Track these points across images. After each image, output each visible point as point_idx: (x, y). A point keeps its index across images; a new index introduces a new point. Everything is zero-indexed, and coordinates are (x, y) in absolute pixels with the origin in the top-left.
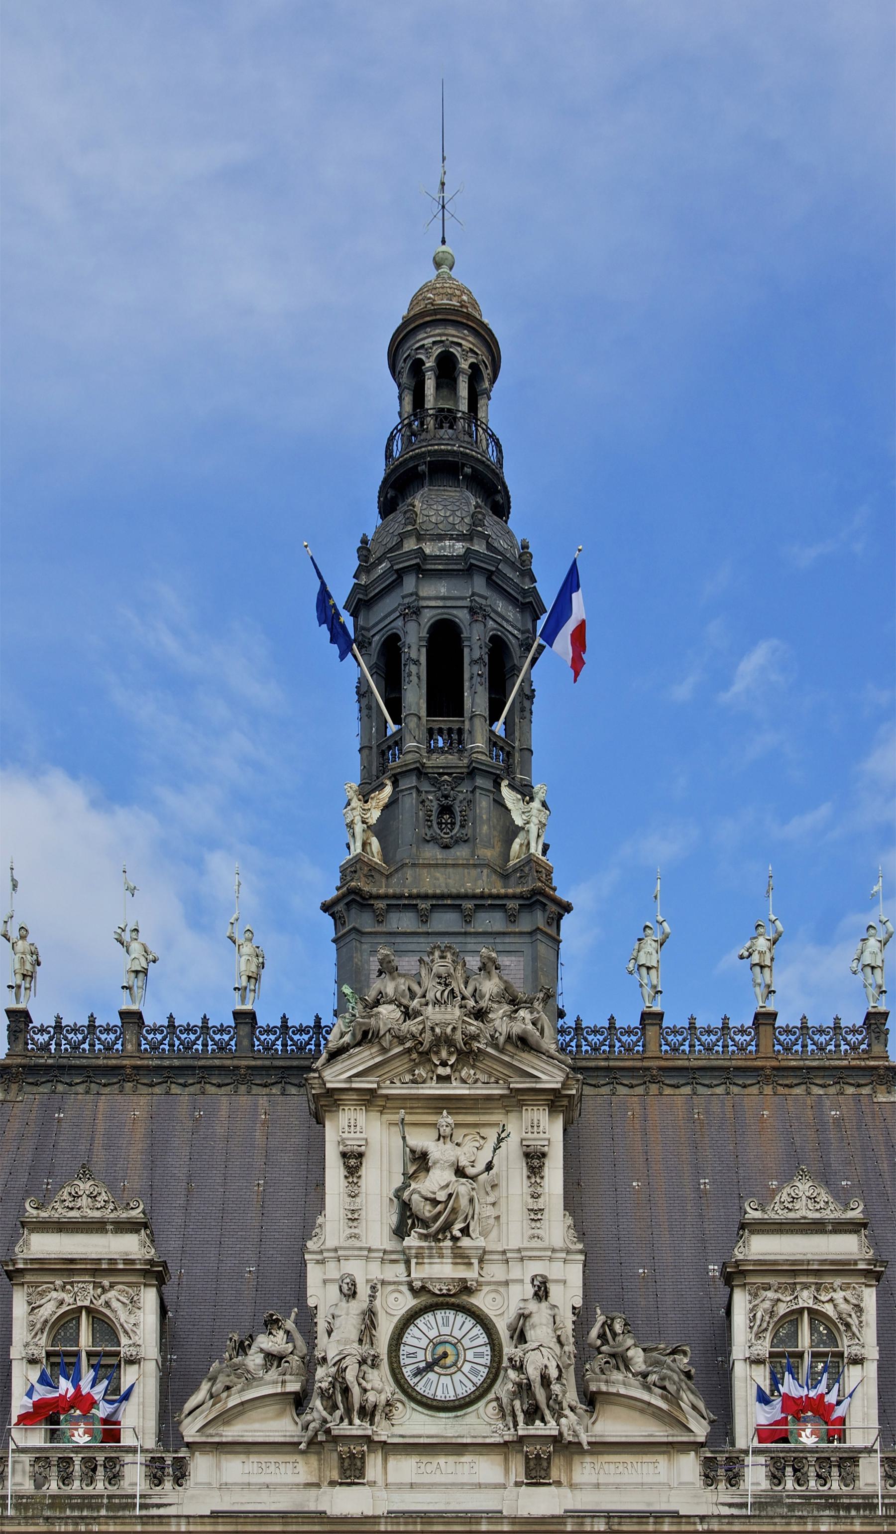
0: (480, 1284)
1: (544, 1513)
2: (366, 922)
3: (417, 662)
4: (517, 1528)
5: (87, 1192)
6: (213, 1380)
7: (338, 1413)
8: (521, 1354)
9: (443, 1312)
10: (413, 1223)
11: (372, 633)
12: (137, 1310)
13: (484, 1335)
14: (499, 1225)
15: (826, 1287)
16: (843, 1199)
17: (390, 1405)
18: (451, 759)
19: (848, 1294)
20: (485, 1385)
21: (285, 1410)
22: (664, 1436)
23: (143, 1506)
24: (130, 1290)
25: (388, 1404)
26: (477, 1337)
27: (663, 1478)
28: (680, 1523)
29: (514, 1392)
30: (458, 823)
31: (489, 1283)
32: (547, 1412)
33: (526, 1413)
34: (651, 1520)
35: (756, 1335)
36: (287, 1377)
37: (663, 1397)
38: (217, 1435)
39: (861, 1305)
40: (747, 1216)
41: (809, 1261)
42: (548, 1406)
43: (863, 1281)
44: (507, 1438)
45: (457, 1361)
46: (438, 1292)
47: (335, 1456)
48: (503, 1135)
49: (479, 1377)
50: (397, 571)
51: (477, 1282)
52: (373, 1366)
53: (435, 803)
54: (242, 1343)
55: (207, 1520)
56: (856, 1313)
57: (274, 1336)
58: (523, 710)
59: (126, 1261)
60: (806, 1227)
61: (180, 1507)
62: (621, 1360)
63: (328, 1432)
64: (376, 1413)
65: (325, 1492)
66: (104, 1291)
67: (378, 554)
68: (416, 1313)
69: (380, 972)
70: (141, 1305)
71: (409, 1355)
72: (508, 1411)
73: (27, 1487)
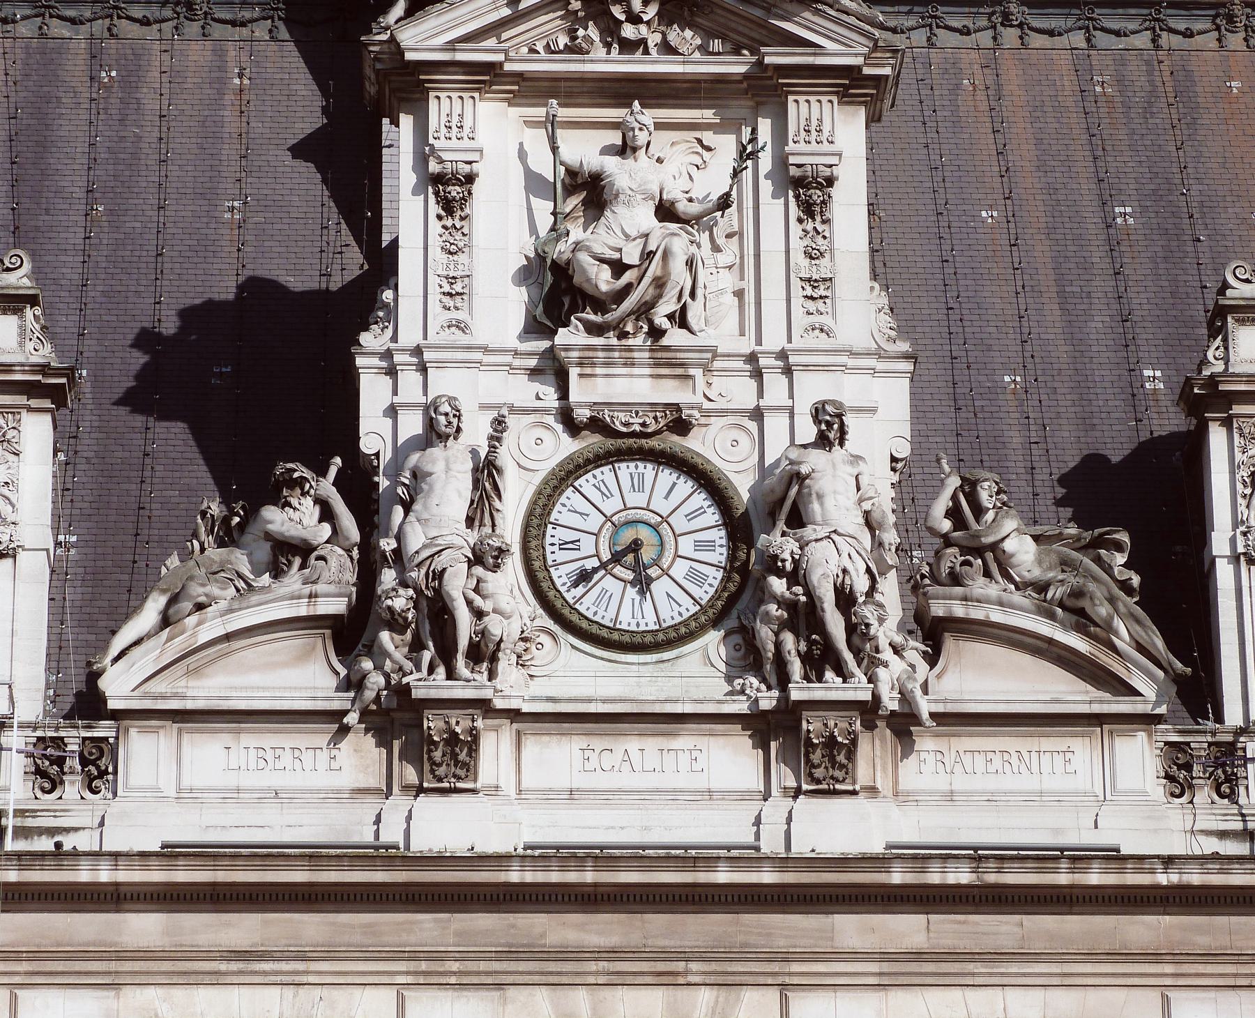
0: (707, 413)
1: (846, 851)
4: (790, 878)
7: (427, 656)
9: (632, 465)
12: (11, 458)
21: (314, 648)
22: (1084, 702)
23: (21, 832)
26: (700, 512)
28: (1122, 871)
31: (723, 413)
32: (848, 656)
33: (805, 658)
34: (1064, 864)
36: (320, 588)
38: (175, 696)
40: (1229, 292)
45: (660, 555)
46: (624, 430)
49: (706, 587)
51: (700, 409)
55: (154, 862)
57: (295, 509)
64: (500, 655)
68: (578, 467)
71: (563, 546)
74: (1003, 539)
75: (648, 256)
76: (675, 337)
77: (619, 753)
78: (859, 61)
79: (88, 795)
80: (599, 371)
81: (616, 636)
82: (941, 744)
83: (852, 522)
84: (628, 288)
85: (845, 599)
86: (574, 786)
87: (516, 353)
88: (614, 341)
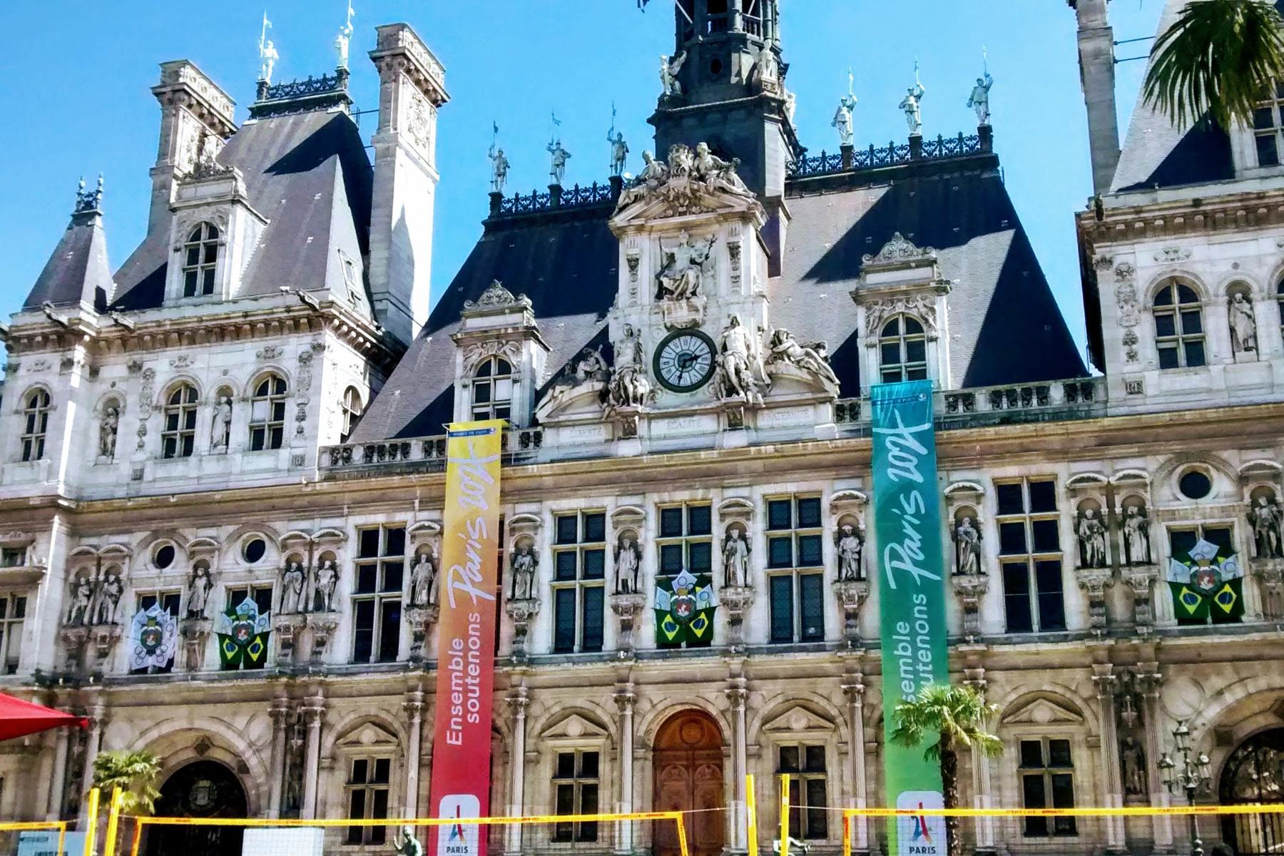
25: (652, 391)
32: (739, 388)
42: (741, 386)
71: (665, 363)
76: (694, 300)
85: (738, 372)
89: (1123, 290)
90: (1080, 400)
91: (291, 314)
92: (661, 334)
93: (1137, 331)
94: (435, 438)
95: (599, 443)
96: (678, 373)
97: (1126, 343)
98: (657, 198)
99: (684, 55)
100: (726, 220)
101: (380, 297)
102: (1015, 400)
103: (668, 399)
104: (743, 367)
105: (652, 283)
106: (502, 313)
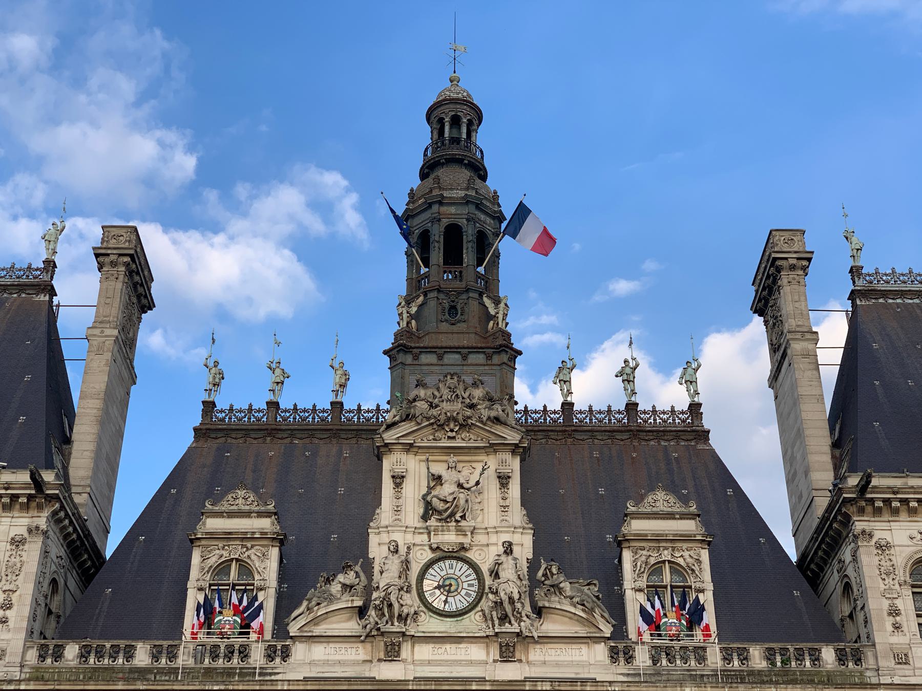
2: (409, 359)
3: (438, 242)
4: (495, 688)
5: (242, 496)
6: (310, 600)
7: (385, 619)
8: (497, 585)
10: (433, 512)
11: (415, 229)
13: (474, 574)
14: (483, 514)
15: (678, 549)
16: (685, 500)
17: (417, 614)
18: (457, 284)
19: (692, 553)
20: (475, 603)
23: (260, 674)
24: (263, 549)
25: (416, 613)
26: (469, 575)
27: (585, 658)
29: (492, 607)
30: (459, 314)
31: (477, 545)
32: (512, 619)
33: (500, 619)
34: (579, 684)
35: (638, 575)
37: (583, 610)
38: (310, 631)
39: (700, 559)
41: (667, 534)
42: (513, 615)
43: (700, 545)
44: (488, 634)
45: (458, 588)
46: (447, 550)
47: (382, 643)
48: (485, 467)
50: (428, 203)
52: (407, 592)
53: (447, 304)
54: (328, 578)
55: (300, 683)
56: (697, 563)
58: (494, 262)
59: (262, 533)
60: (664, 516)
61: (284, 675)
62: (556, 588)
63: (379, 629)
65: (375, 666)
66: (248, 549)
67: (419, 196)
69: (417, 386)
70: (269, 557)
72: (489, 617)
73: (190, 662)
74: (560, 583)
75: (455, 498)
76: (463, 523)
77: (443, 649)
78: (518, 442)
79: (283, 662)
80: (440, 533)
81: (444, 613)
82: (541, 646)
83: (514, 577)
84: (448, 508)
86: (430, 659)
87: (416, 528)
88: (444, 524)
89: (883, 563)
90: (850, 664)
91: (9, 492)
92: (425, 555)
93: (899, 603)
94: (165, 643)
95: (355, 663)
96: (444, 598)
97: (890, 614)
98: (428, 419)
99: (421, 298)
100: (495, 451)
101: (79, 490)
102: (789, 660)
103: (430, 624)
104: (516, 596)
105: (417, 501)
106: (247, 514)
